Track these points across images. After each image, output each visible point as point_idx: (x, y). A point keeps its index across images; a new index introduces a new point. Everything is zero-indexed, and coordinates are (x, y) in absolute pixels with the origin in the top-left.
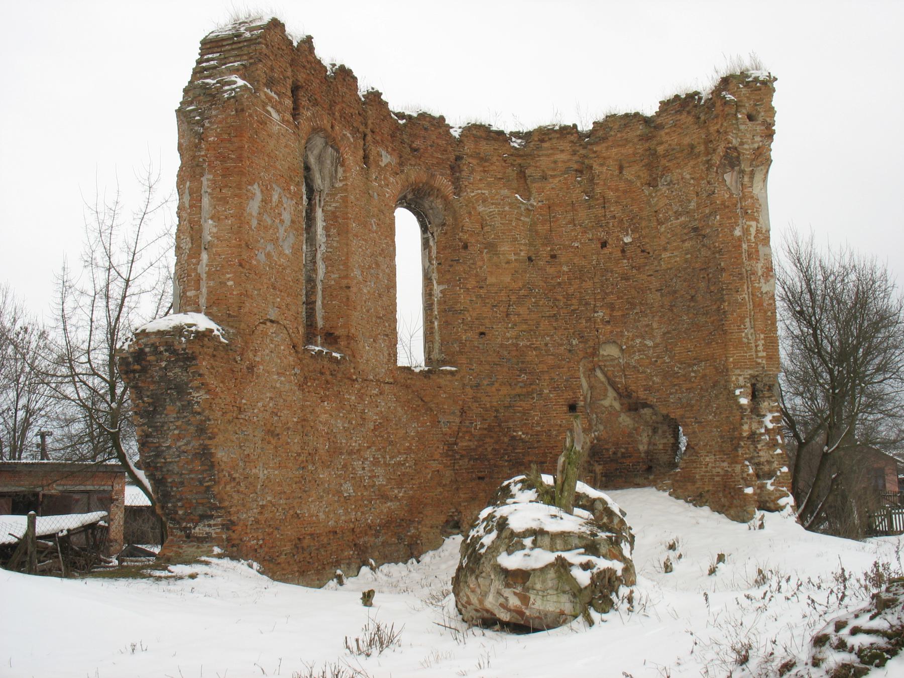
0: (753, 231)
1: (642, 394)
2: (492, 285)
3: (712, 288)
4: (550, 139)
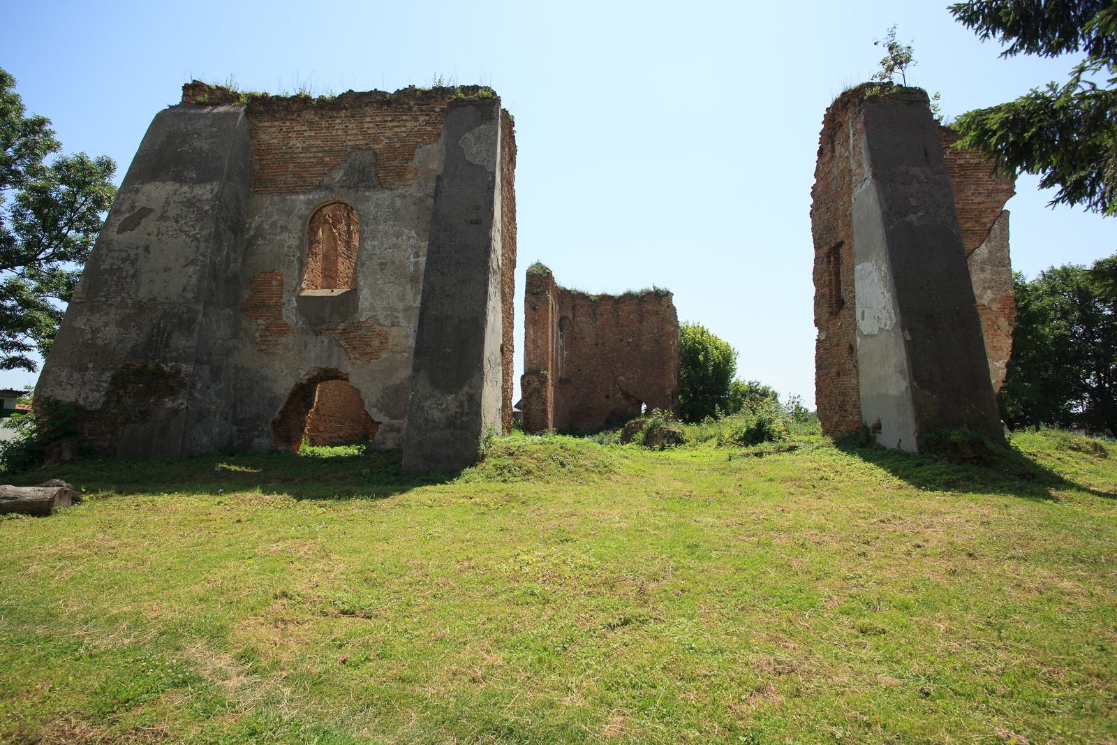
1: (632, 394)
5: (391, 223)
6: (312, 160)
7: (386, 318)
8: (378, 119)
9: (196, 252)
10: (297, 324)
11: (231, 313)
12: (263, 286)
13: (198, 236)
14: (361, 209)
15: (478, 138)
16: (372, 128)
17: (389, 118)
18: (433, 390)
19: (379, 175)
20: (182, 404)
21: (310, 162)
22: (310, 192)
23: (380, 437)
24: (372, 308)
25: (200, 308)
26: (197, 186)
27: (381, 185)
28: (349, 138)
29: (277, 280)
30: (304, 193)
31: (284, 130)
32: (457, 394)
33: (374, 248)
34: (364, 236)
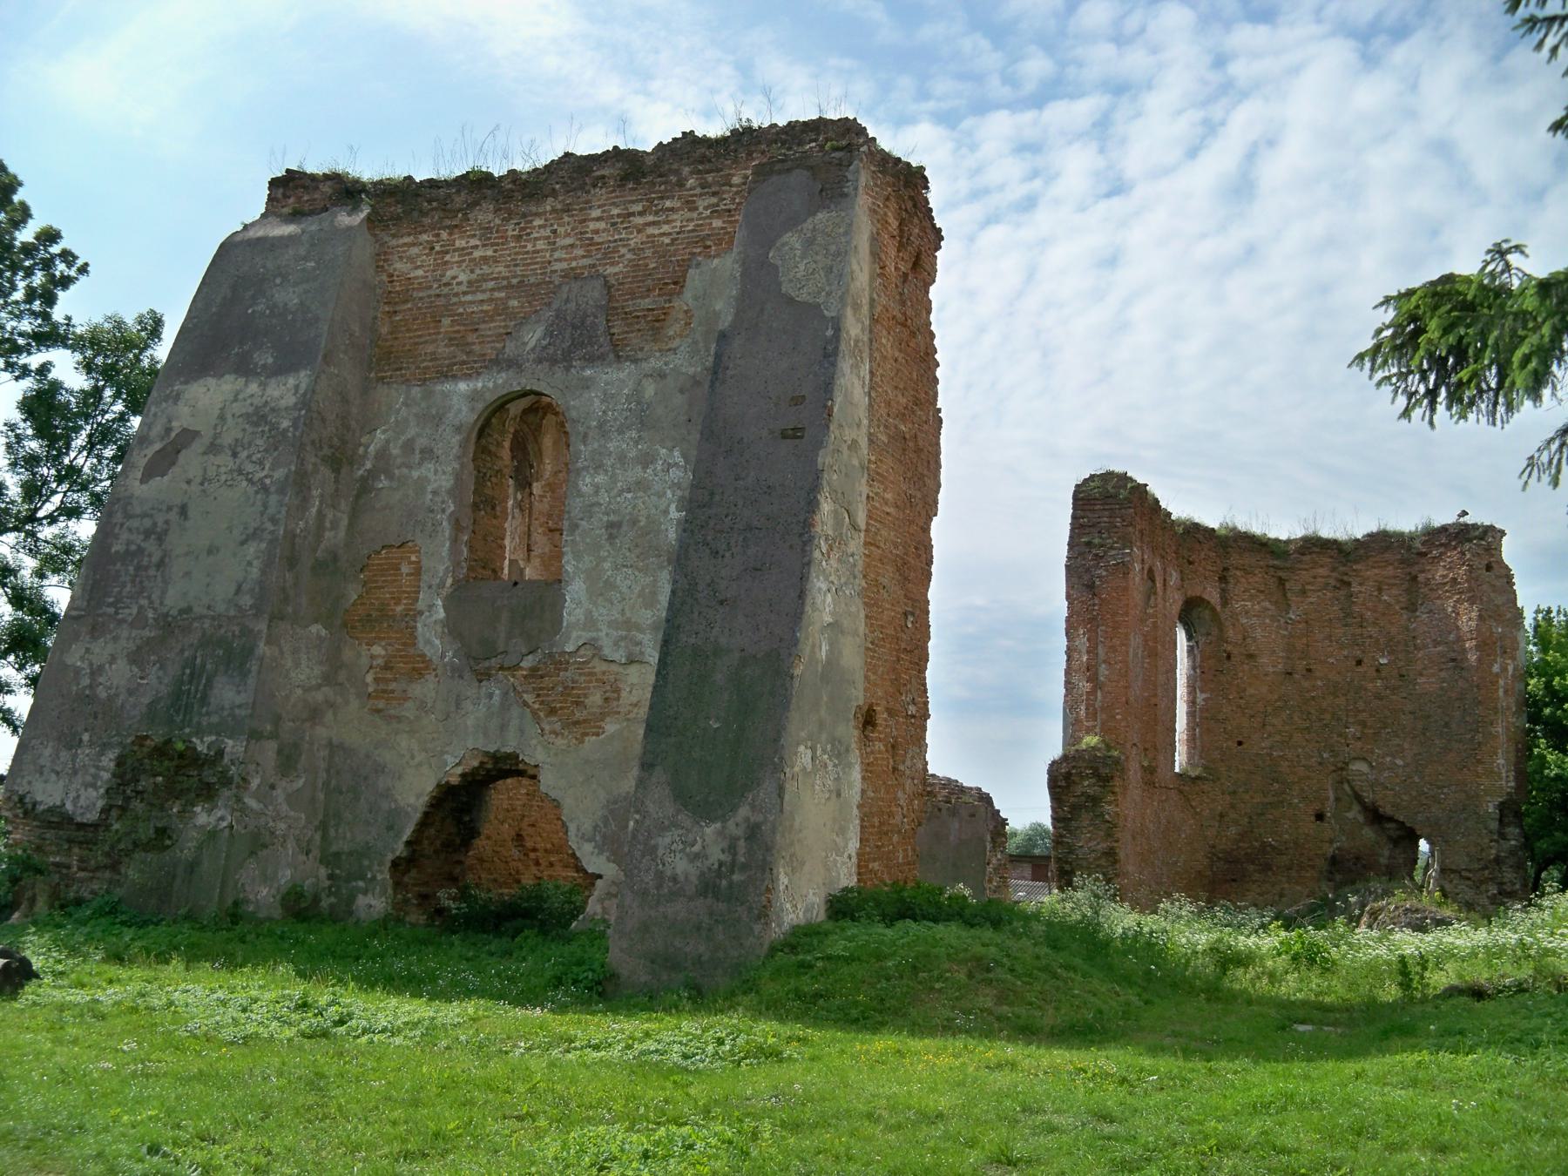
0: (1510, 668)
2: (1251, 696)
5: (634, 434)
6: (485, 307)
7: (616, 644)
8: (615, 211)
9: (262, 514)
10: (443, 656)
11: (323, 632)
12: (383, 575)
13: (268, 481)
14: (574, 407)
15: (810, 243)
16: (604, 231)
17: (638, 208)
18: (679, 811)
19: (612, 331)
20: (222, 819)
21: (482, 311)
22: (479, 374)
23: (599, 909)
24: (590, 622)
25: (262, 626)
26: (273, 381)
27: (618, 352)
28: (557, 255)
29: (411, 563)
30: (468, 377)
31: (437, 248)
32: (724, 821)
33: (597, 489)
34: (579, 465)
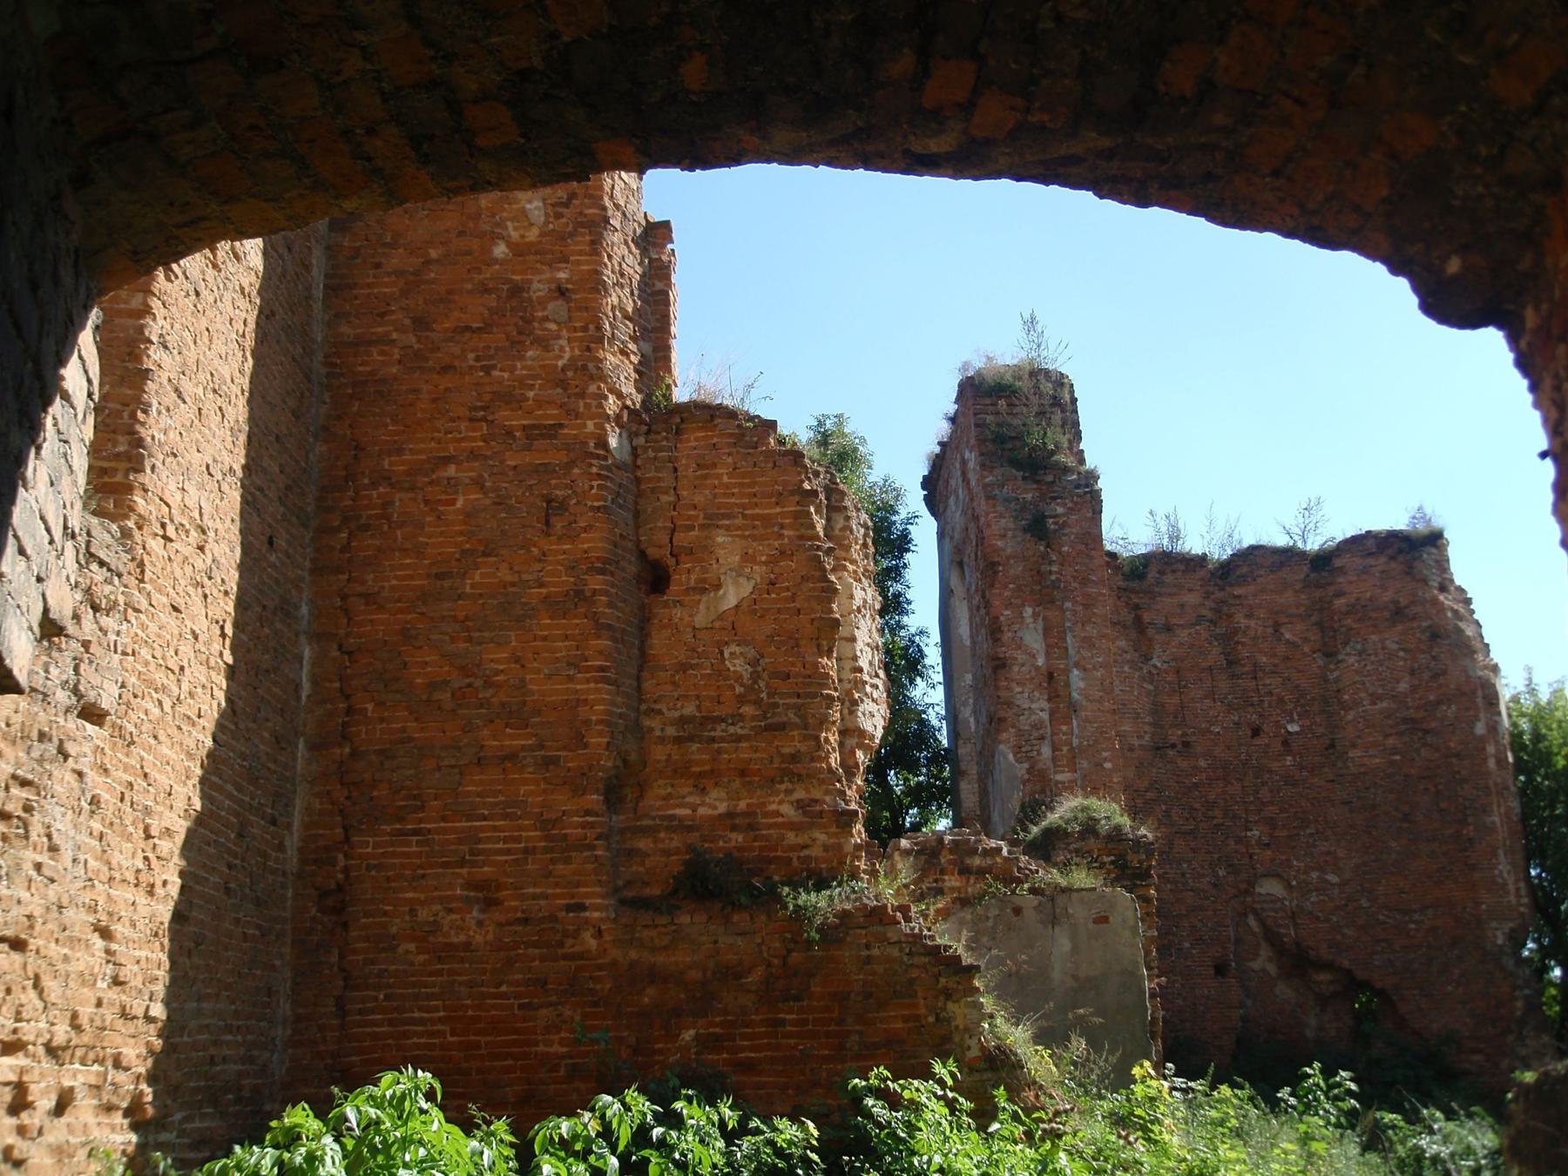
3: (1443, 805)
4: (1174, 571)
